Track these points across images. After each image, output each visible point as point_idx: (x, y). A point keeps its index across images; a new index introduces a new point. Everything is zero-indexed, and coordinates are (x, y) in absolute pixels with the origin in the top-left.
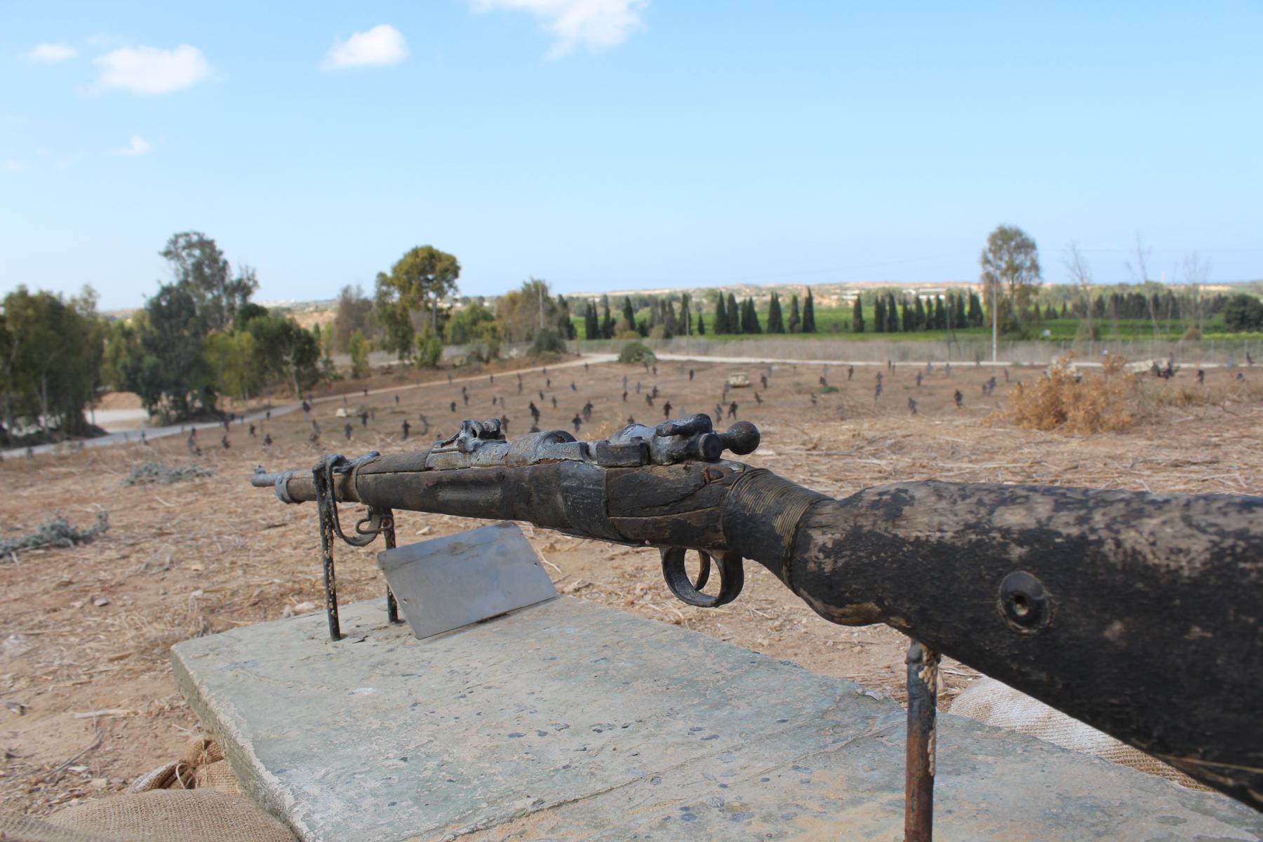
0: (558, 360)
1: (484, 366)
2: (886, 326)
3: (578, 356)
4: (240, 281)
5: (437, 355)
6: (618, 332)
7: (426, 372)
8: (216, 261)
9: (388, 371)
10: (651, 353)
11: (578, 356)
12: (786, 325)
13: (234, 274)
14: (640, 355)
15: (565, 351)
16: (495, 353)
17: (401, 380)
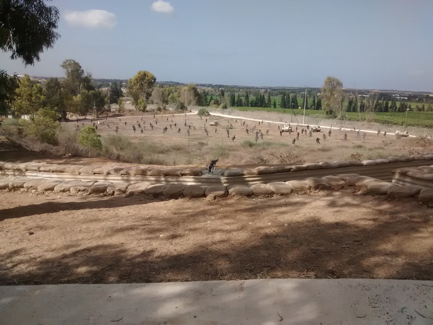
0: (183, 112)
1: (159, 112)
2: (352, 110)
3: (191, 111)
4: (86, 77)
5: (145, 107)
6: (211, 105)
7: (141, 112)
8: (78, 70)
9: (130, 111)
10: (208, 113)
11: (191, 111)
12: (309, 106)
13: (85, 75)
14: (204, 113)
15: (187, 110)
16: (165, 109)
17: (133, 114)
